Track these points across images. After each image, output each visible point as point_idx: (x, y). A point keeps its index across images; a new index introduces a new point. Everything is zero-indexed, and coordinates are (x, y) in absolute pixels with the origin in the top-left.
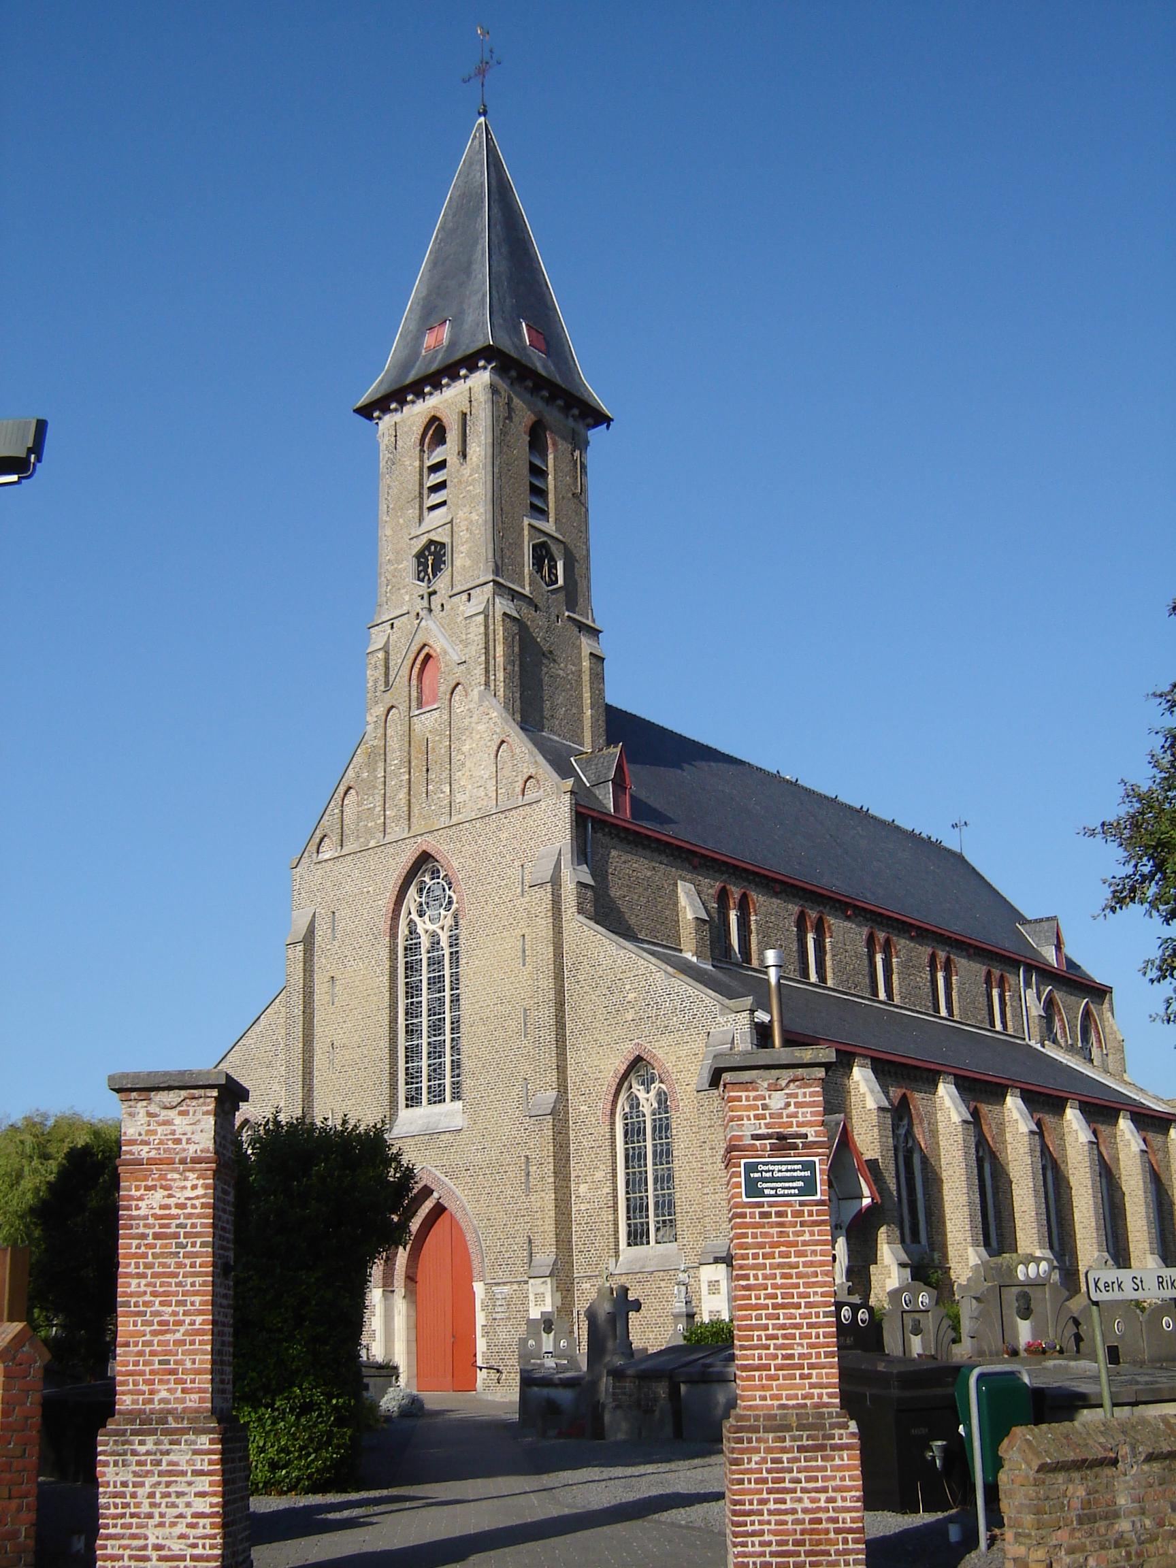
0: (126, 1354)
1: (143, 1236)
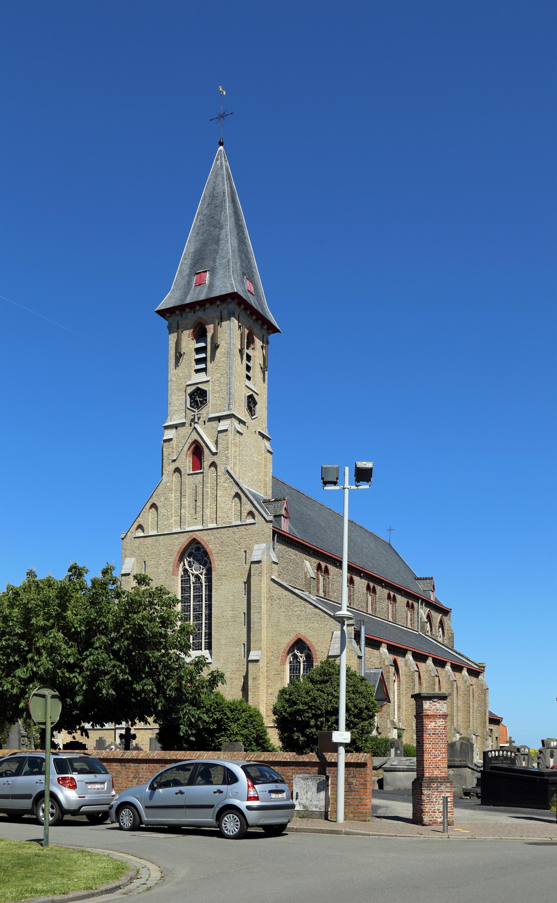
0: (426, 763)
1: (430, 734)
